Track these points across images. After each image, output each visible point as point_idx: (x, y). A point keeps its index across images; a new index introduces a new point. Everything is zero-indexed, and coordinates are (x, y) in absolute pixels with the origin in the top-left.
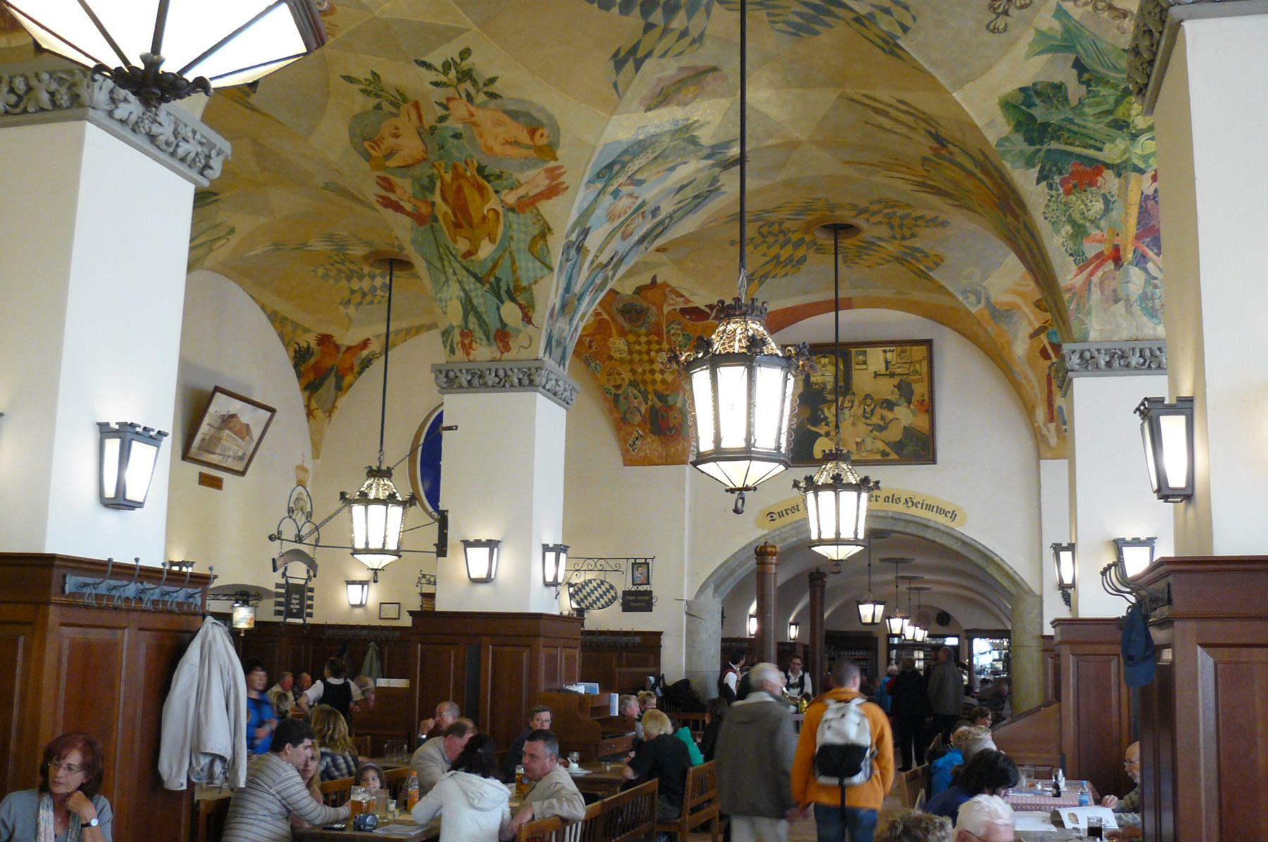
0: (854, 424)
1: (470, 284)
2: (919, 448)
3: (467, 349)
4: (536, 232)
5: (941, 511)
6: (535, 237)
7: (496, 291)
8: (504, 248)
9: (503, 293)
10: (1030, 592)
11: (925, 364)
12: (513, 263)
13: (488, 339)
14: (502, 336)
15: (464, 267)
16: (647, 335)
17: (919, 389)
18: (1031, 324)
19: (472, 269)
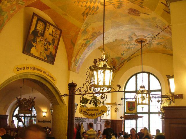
0: (42, 46)
2: (51, 59)
5: (53, 79)
11: (59, 35)
17: (56, 42)
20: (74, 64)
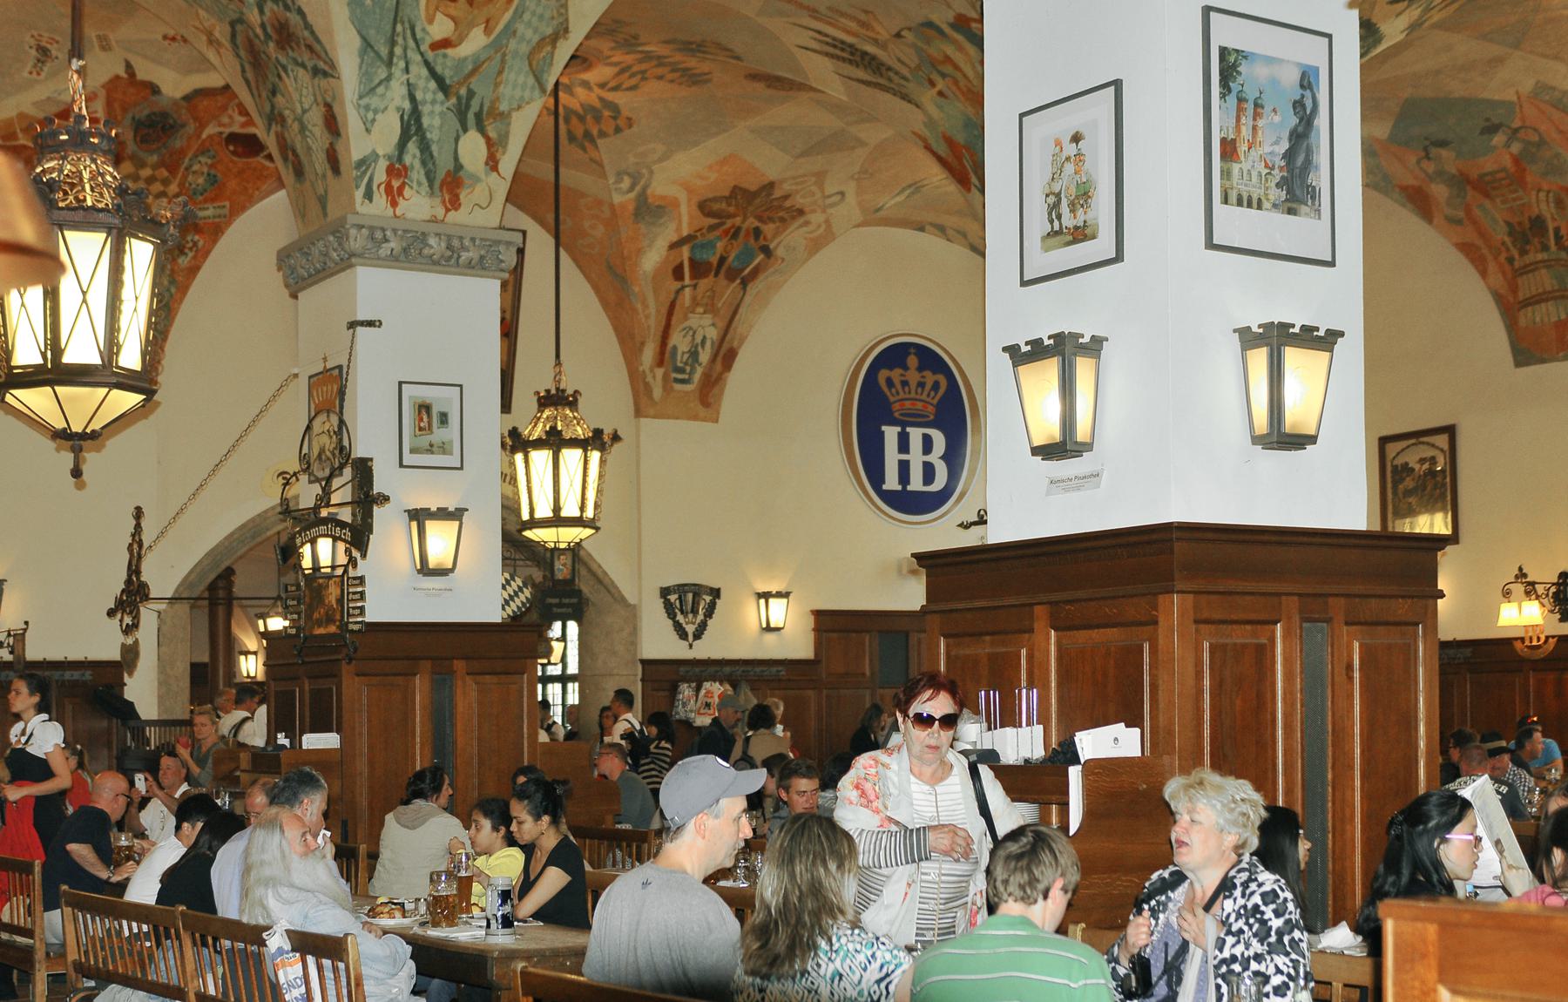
1: (427, 91)
3: (394, 196)
4: (549, 31)
6: (543, 39)
7: (461, 113)
8: (497, 46)
9: (471, 116)
10: (622, 600)
12: (500, 72)
13: (431, 186)
14: (451, 185)
15: (427, 63)
16: (155, 167)
18: (679, 229)
19: (439, 69)
20: (665, 377)
